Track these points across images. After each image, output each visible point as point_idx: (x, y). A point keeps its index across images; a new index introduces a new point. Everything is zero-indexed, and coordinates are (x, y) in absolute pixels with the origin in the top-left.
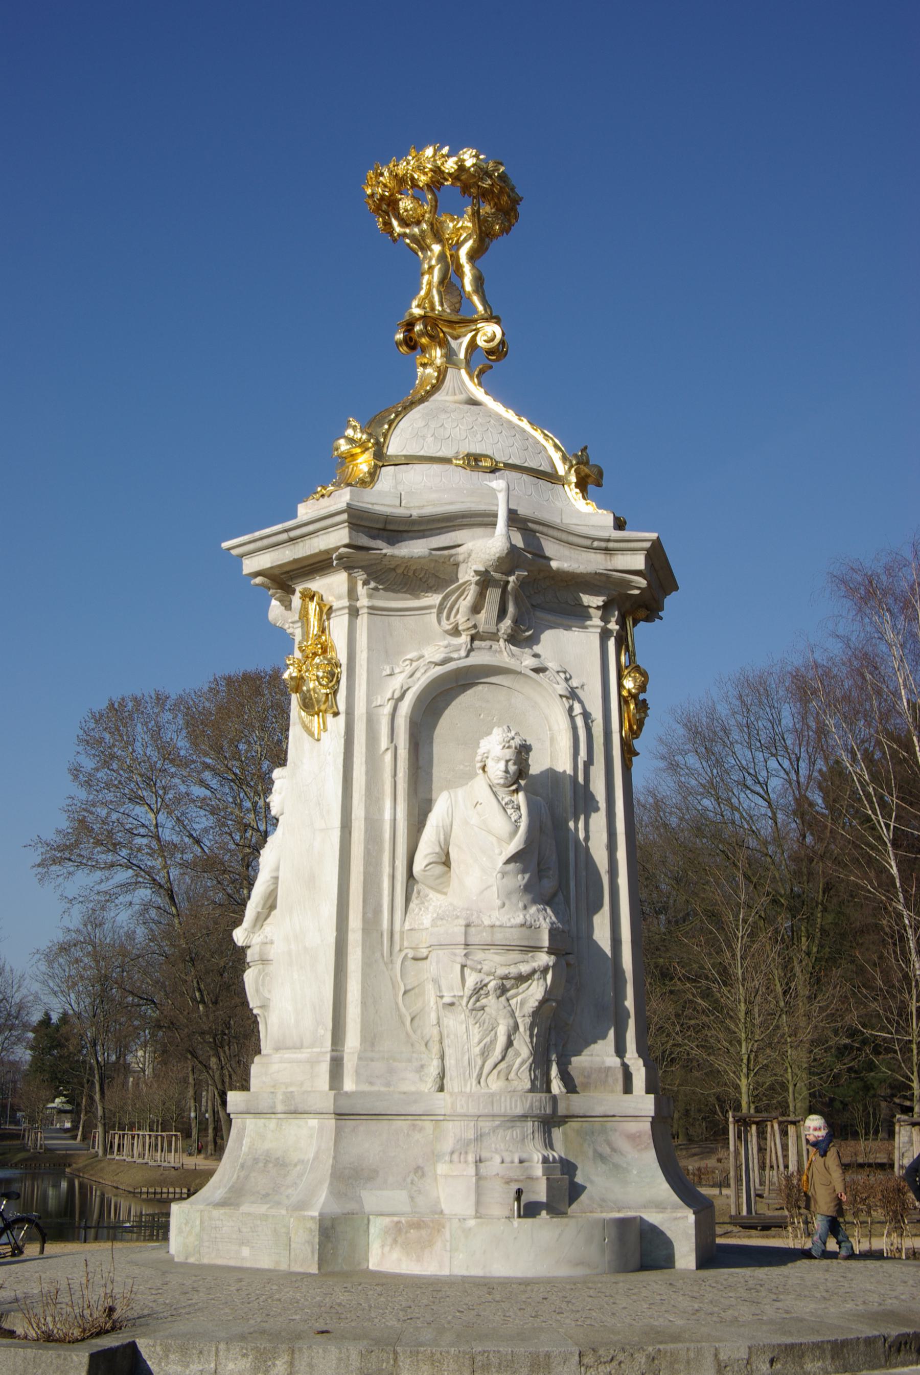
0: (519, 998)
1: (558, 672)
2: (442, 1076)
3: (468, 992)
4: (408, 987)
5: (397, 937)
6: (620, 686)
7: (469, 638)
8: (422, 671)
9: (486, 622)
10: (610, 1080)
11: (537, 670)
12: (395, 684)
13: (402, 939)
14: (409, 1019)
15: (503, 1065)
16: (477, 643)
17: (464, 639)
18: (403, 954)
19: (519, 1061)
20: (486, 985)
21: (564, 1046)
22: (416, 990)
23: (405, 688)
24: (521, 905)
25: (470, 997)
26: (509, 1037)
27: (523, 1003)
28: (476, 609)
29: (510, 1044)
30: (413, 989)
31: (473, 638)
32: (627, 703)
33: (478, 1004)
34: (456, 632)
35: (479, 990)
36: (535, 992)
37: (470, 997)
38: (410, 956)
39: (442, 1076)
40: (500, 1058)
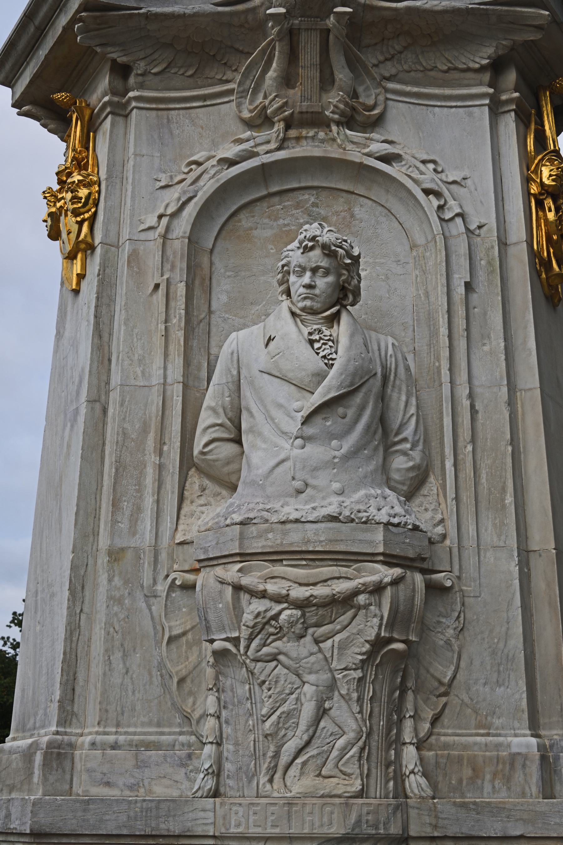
0: (337, 638)
1: (424, 162)
2: (217, 773)
3: (245, 633)
4: (175, 632)
5: (163, 556)
6: (527, 181)
7: (282, 125)
8: (212, 172)
9: (303, 98)
10: (519, 776)
11: (387, 159)
12: (172, 197)
13: (172, 559)
14: (175, 680)
15: (312, 751)
16: (293, 133)
17: (279, 126)
18: (170, 579)
19: (341, 743)
20: (276, 617)
21: (435, 721)
22: (190, 636)
23: (183, 199)
24: (336, 486)
25: (250, 639)
26: (320, 703)
27: (343, 647)
28: (287, 80)
29: (322, 712)
30: (184, 634)
31: (288, 127)
32: (540, 205)
33: (265, 650)
34: (261, 120)
35: (264, 626)
36: (367, 626)
37: (250, 639)
38: (178, 583)
39: (217, 773)
40: (306, 737)
